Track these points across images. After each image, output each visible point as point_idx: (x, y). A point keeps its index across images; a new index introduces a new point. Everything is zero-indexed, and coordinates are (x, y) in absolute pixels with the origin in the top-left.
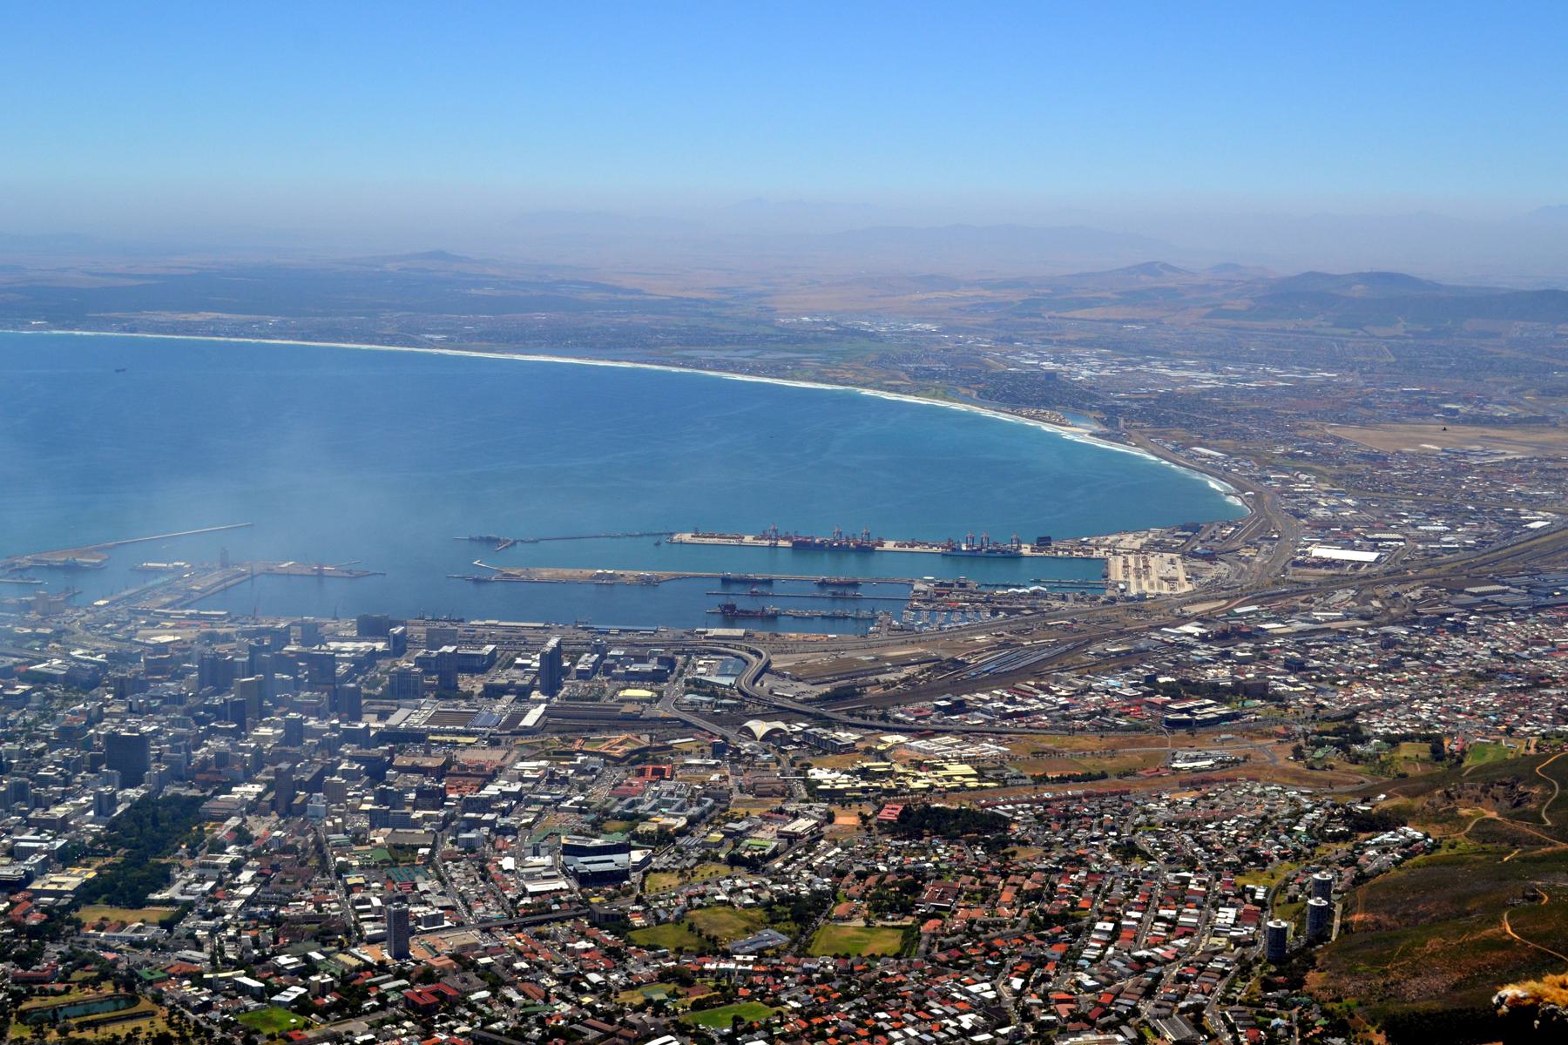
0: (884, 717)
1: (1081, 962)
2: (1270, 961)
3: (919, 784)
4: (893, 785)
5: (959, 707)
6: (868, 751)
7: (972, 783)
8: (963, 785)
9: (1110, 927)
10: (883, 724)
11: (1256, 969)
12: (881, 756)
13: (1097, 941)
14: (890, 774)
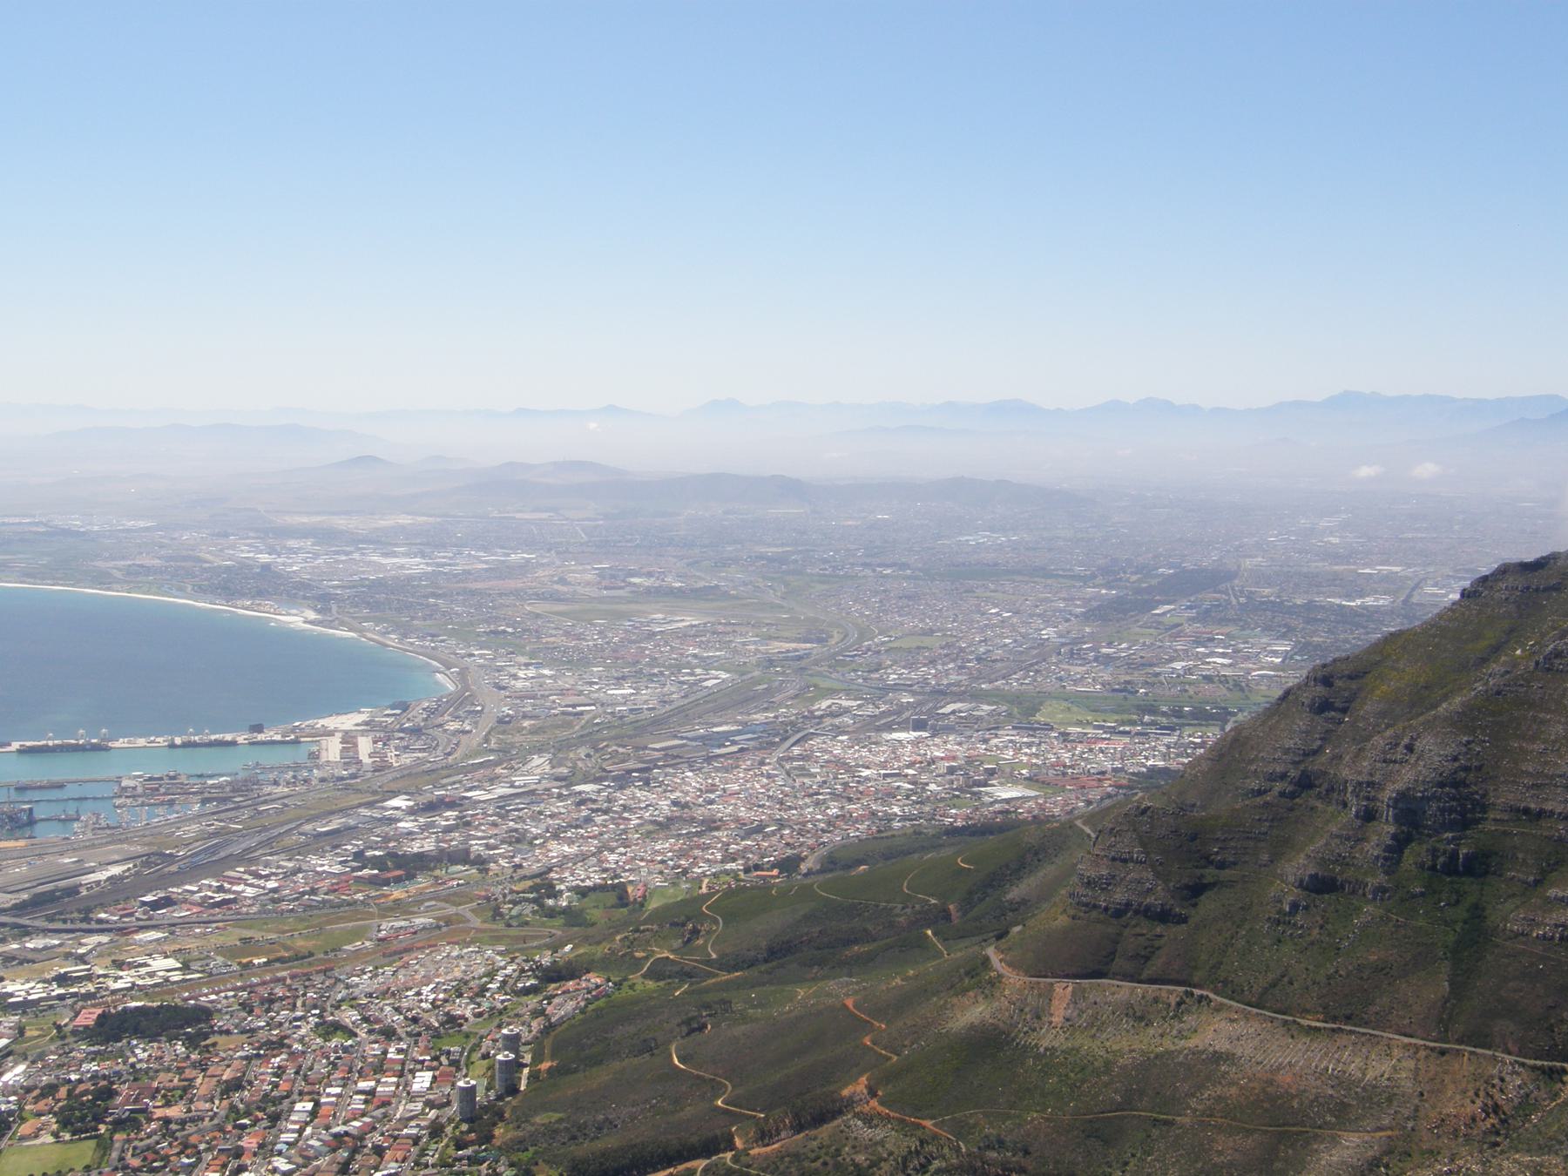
0: (87, 920)
1: (278, 1147)
2: (462, 1121)
3: (120, 985)
4: (91, 987)
5: (168, 902)
6: (68, 956)
7: (176, 977)
8: (167, 980)
9: (309, 1106)
10: (84, 926)
11: (449, 1129)
12: (82, 959)
13: (295, 1122)
14: (89, 978)
